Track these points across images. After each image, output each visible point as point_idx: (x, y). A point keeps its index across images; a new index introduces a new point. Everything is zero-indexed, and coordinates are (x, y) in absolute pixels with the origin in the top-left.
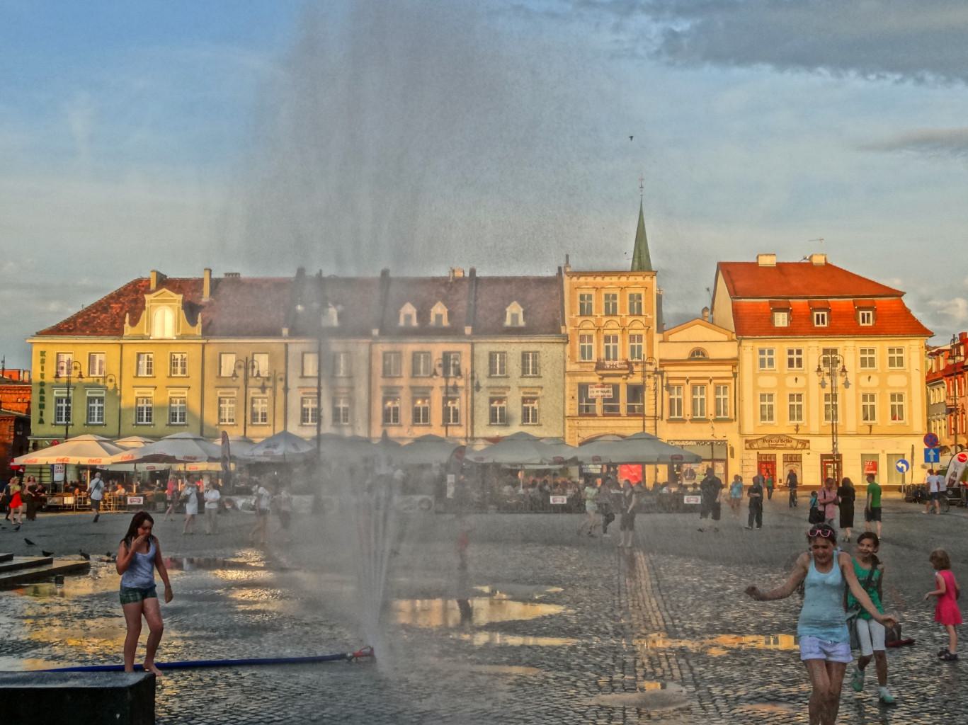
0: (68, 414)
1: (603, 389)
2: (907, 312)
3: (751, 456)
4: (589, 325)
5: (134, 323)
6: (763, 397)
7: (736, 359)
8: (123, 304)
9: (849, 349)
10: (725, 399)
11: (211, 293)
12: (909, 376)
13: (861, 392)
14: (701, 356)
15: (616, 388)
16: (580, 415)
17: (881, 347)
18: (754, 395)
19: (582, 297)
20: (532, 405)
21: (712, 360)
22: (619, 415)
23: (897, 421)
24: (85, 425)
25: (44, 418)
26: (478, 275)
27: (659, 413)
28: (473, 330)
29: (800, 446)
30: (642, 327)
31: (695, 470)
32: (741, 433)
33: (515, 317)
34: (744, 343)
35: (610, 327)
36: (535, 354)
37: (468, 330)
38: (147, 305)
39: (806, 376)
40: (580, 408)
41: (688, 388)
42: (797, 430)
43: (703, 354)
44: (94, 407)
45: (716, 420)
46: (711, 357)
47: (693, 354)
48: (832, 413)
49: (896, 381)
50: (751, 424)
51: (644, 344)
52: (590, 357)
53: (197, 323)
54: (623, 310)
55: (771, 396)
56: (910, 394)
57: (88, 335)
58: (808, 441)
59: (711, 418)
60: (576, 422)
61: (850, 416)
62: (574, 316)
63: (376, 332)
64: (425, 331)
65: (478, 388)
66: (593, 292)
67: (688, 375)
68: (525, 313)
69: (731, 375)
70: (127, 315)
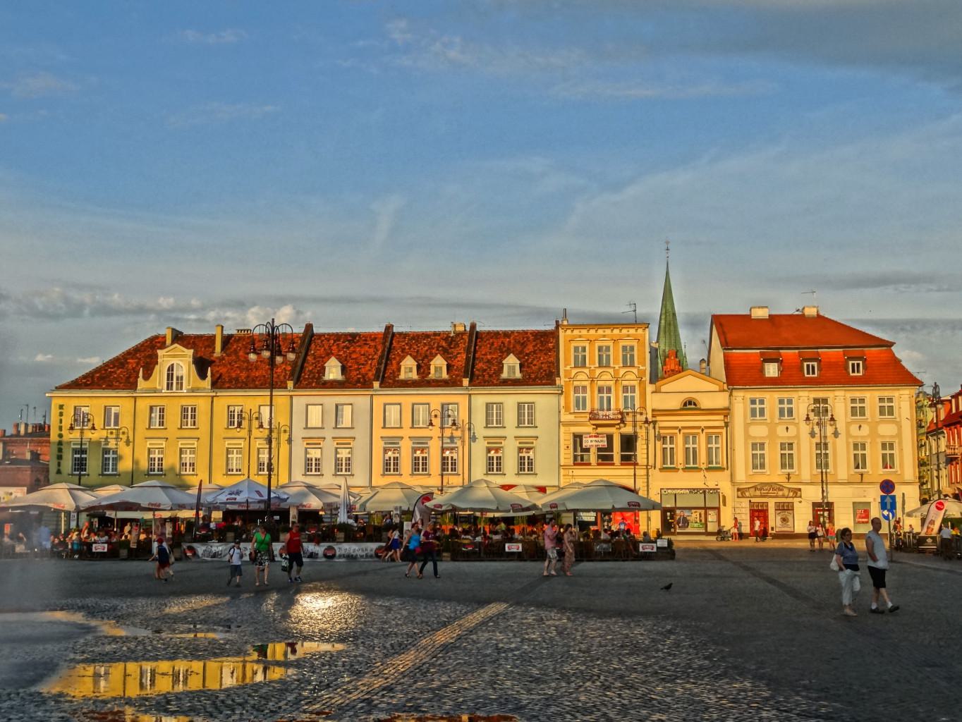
1: (596, 439)
2: (897, 362)
3: (743, 505)
4: (582, 377)
5: (147, 377)
6: (754, 446)
7: (728, 409)
8: (140, 359)
9: (839, 399)
10: (716, 448)
11: (223, 348)
13: (851, 440)
14: (693, 406)
15: (610, 438)
16: (575, 464)
17: (871, 396)
18: (746, 444)
19: (576, 349)
20: (528, 455)
21: (703, 410)
22: (613, 464)
23: (889, 470)
24: (99, 475)
25: (61, 468)
26: (478, 329)
27: (651, 462)
28: (470, 382)
29: (791, 494)
30: (635, 378)
31: (688, 518)
32: (732, 481)
34: (735, 393)
35: (603, 378)
36: (531, 406)
39: (797, 425)
40: (575, 457)
42: (789, 479)
43: (695, 404)
44: (109, 458)
45: (708, 469)
46: (702, 408)
47: (685, 405)
48: (822, 461)
49: (887, 430)
50: (742, 474)
52: (584, 407)
55: (762, 445)
56: (900, 443)
57: (104, 389)
58: (800, 490)
59: (703, 467)
60: (571, 471)
61: (841, 465)
62: (568, 368)
63: (376, 384)
64: (424, 382)
65: (473, 438)
66: (587, 344)
67: (680, 425)
68: (521, 366)
69: (722, 424)
70: (141, 369)
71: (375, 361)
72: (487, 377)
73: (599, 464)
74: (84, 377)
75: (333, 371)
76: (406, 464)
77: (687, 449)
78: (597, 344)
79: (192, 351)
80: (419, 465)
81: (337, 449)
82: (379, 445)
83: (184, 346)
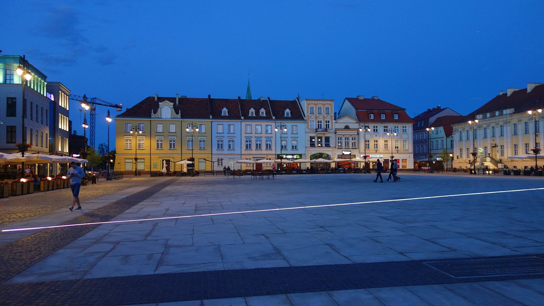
5: (155, 113)
12: (408, 136)
33: (287, 114)
37: (274, 118)
41: (344, 138)
51: (330, 124)
54: (324, 112)
63: (243, 118)
64: (258, 117)
71: (240, 109)
75: (225, 111)
76: (254, 147)
78: (318, 106)
79: (172, 104)
80: (259, 147)
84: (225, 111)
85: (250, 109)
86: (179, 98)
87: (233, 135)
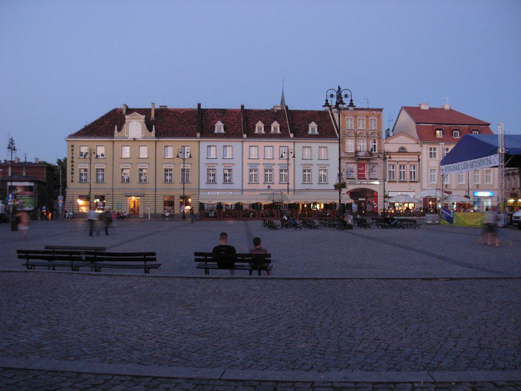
0: (309, 178)
5: (119, 130)
11: (155, 115)
22: (365, 179)
37: (292, 135)
38: (126, 121)
41: (398, 166)
43: (404, 150)
46: (408, 151)
53: (152, 130)
57: (96, 136)
59: (408, 181)
63: (245, 136)
64: (268, 135)
69: (417, 160)
71: (242, 124)
72: (301, 133)
73: (359, 179)
74: (83, 130)
75: (219, 127)
77: (401, 172)
79: (144, 116)
81: (224, 169)
82: (246, 169)
83: (141, 114)
84: (219, 127)
85: (257, 122)
86: (156, 110)
87: (231, 161)
